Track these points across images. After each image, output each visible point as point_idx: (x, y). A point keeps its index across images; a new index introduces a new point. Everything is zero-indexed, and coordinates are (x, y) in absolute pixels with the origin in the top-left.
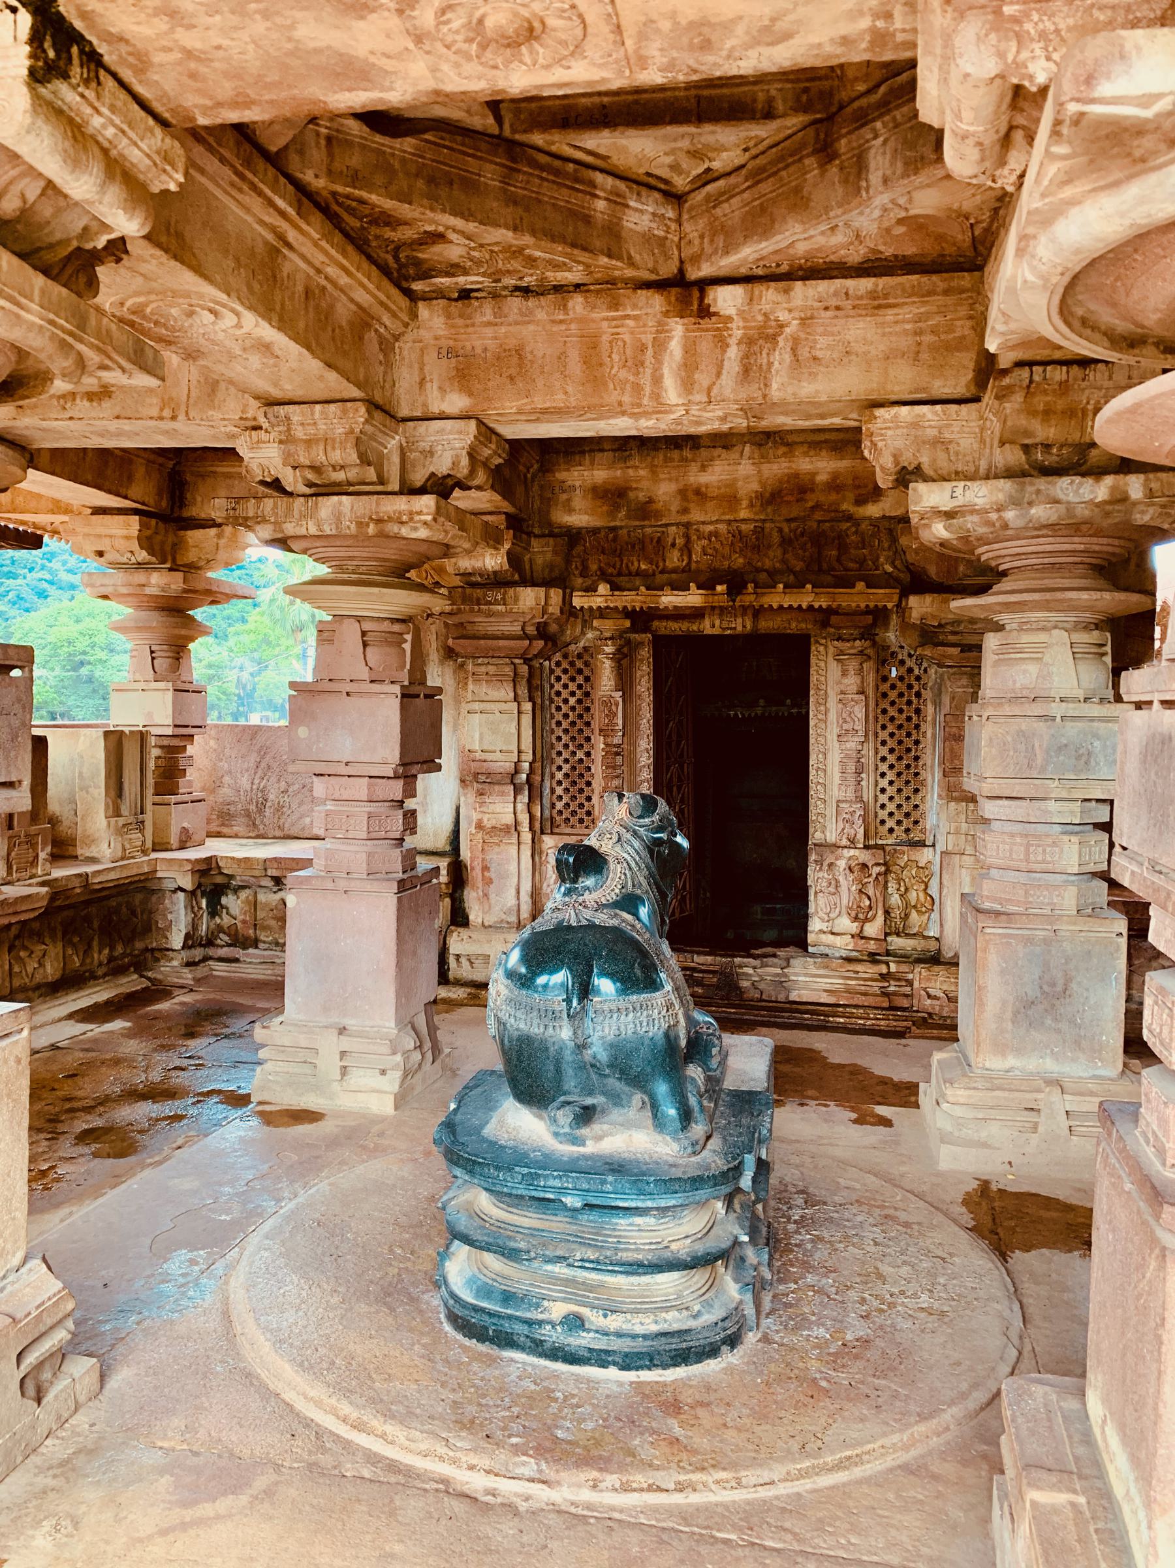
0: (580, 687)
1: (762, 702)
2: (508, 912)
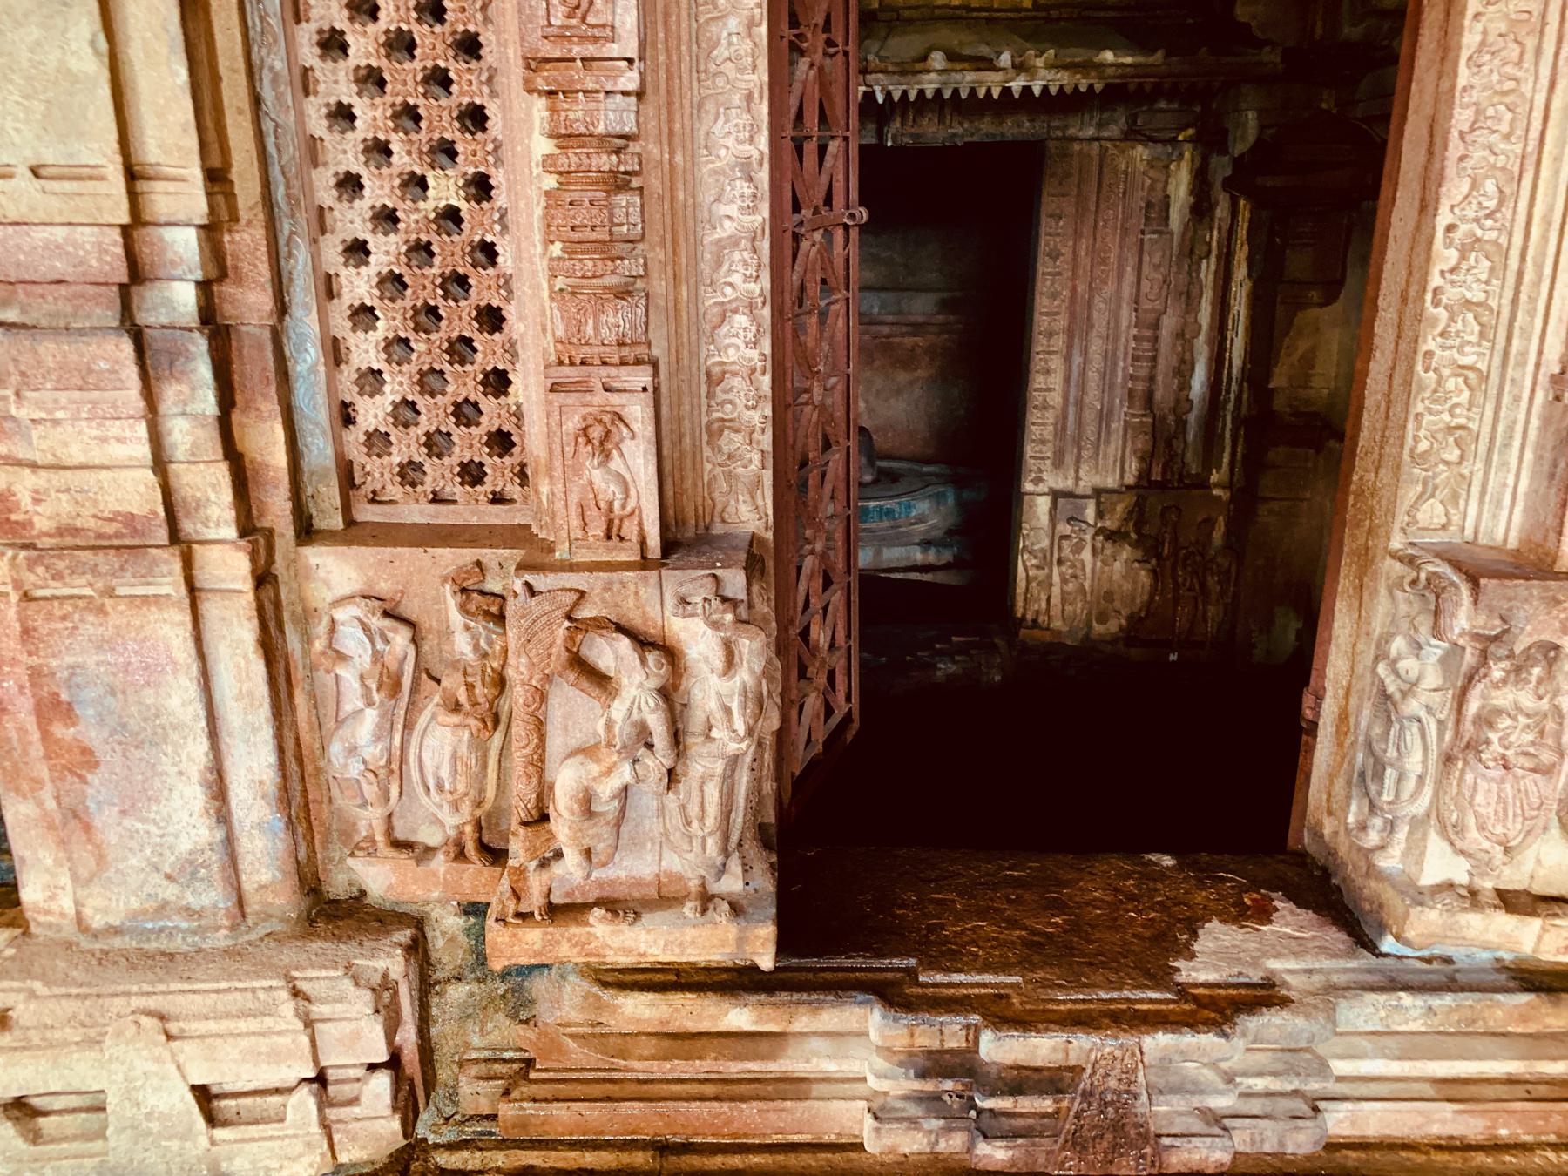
1: (937, 60)
2: (188, 871)
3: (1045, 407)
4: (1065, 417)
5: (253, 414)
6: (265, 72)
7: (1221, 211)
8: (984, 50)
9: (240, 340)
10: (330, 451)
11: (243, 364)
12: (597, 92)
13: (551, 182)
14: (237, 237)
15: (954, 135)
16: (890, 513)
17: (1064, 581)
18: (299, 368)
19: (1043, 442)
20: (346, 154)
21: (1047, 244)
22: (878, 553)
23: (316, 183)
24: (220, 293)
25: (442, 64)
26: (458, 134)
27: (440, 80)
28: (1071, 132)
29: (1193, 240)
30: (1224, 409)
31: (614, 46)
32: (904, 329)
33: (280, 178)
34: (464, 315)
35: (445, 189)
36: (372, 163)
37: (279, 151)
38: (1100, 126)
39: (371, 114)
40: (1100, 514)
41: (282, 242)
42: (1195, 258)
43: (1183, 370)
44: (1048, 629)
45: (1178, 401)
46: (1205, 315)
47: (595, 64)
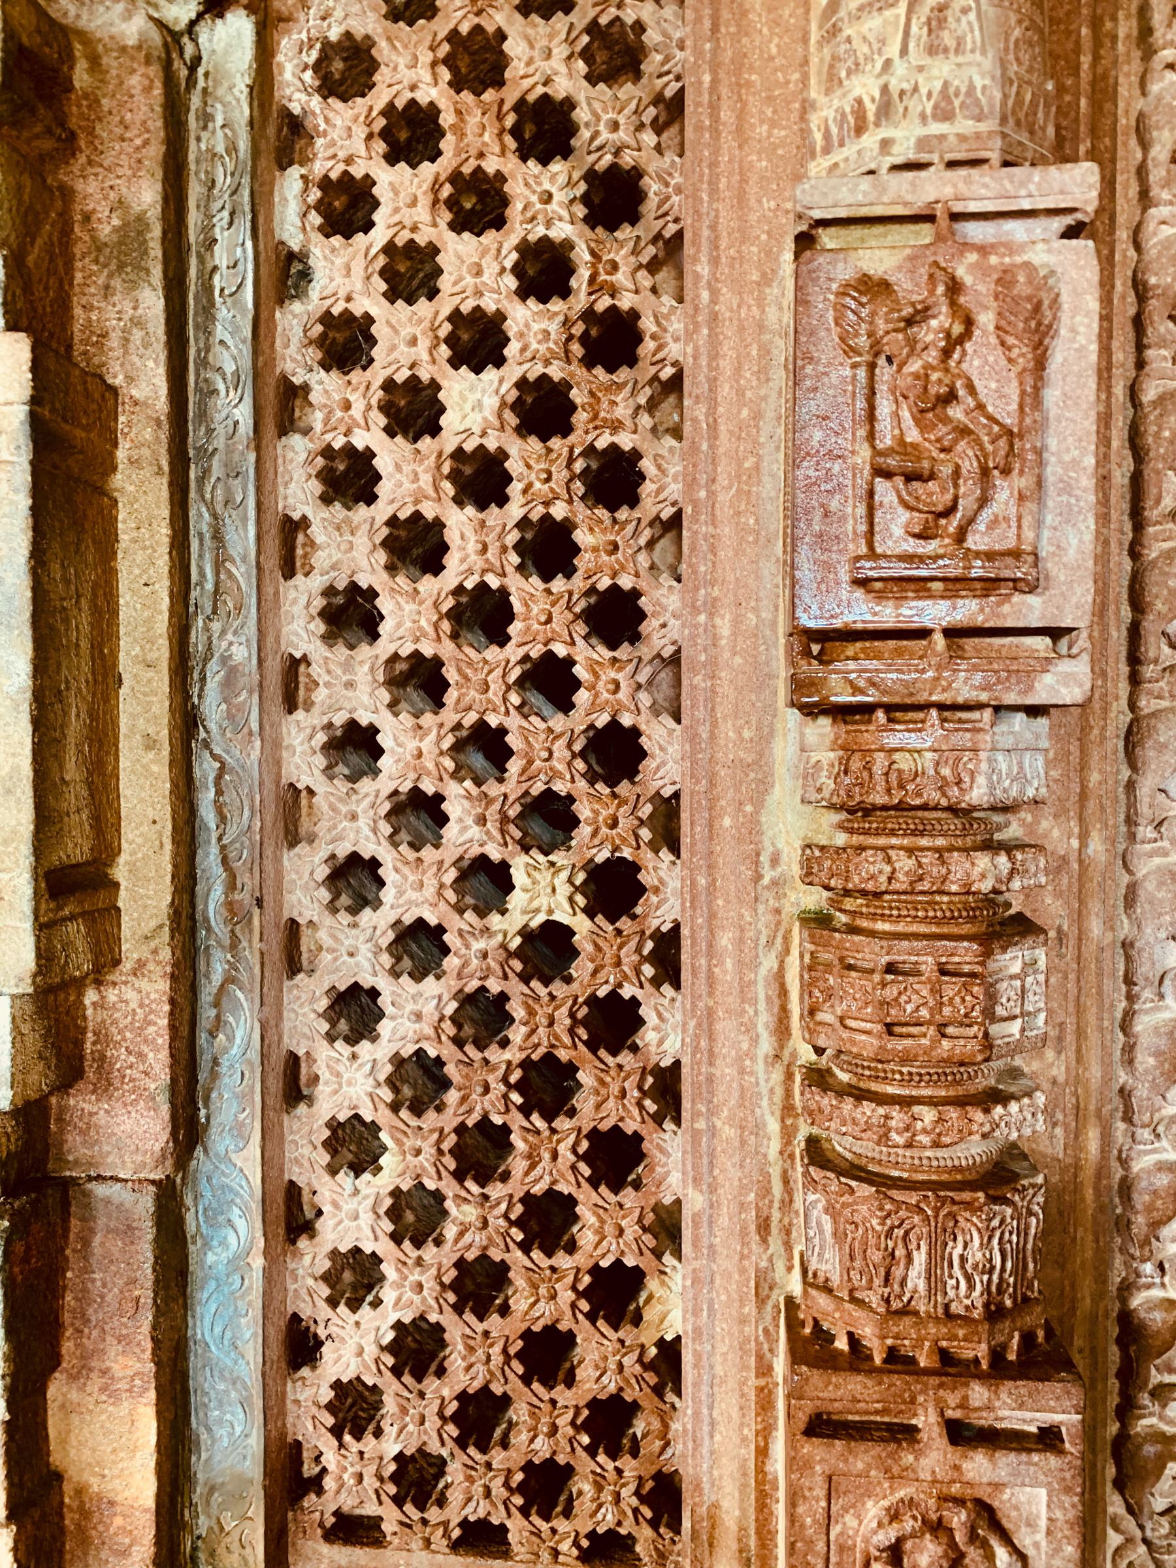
0: (543, 272)
5: (95, 1383)
6: (213, 665)
9: (88, 1218)
10: (255, 1443)
11: (87, 1270)
12: (980, 706)
13: (814, 898)
14: (112, 995)
18: (210, 1258)
20: (353, 820)
23: (290, 877)
24: (62, 1110)
25: (561, 650)
26: (582, 784)
27: (551, 680)
31: (1031, 599)
33: (218, 870)
34: (564, 1149)
35: (544, 891)
36: (404, 836)
37: (222, 819)
39: (412, 745)
41: (206, 995)
47: (970, 643)
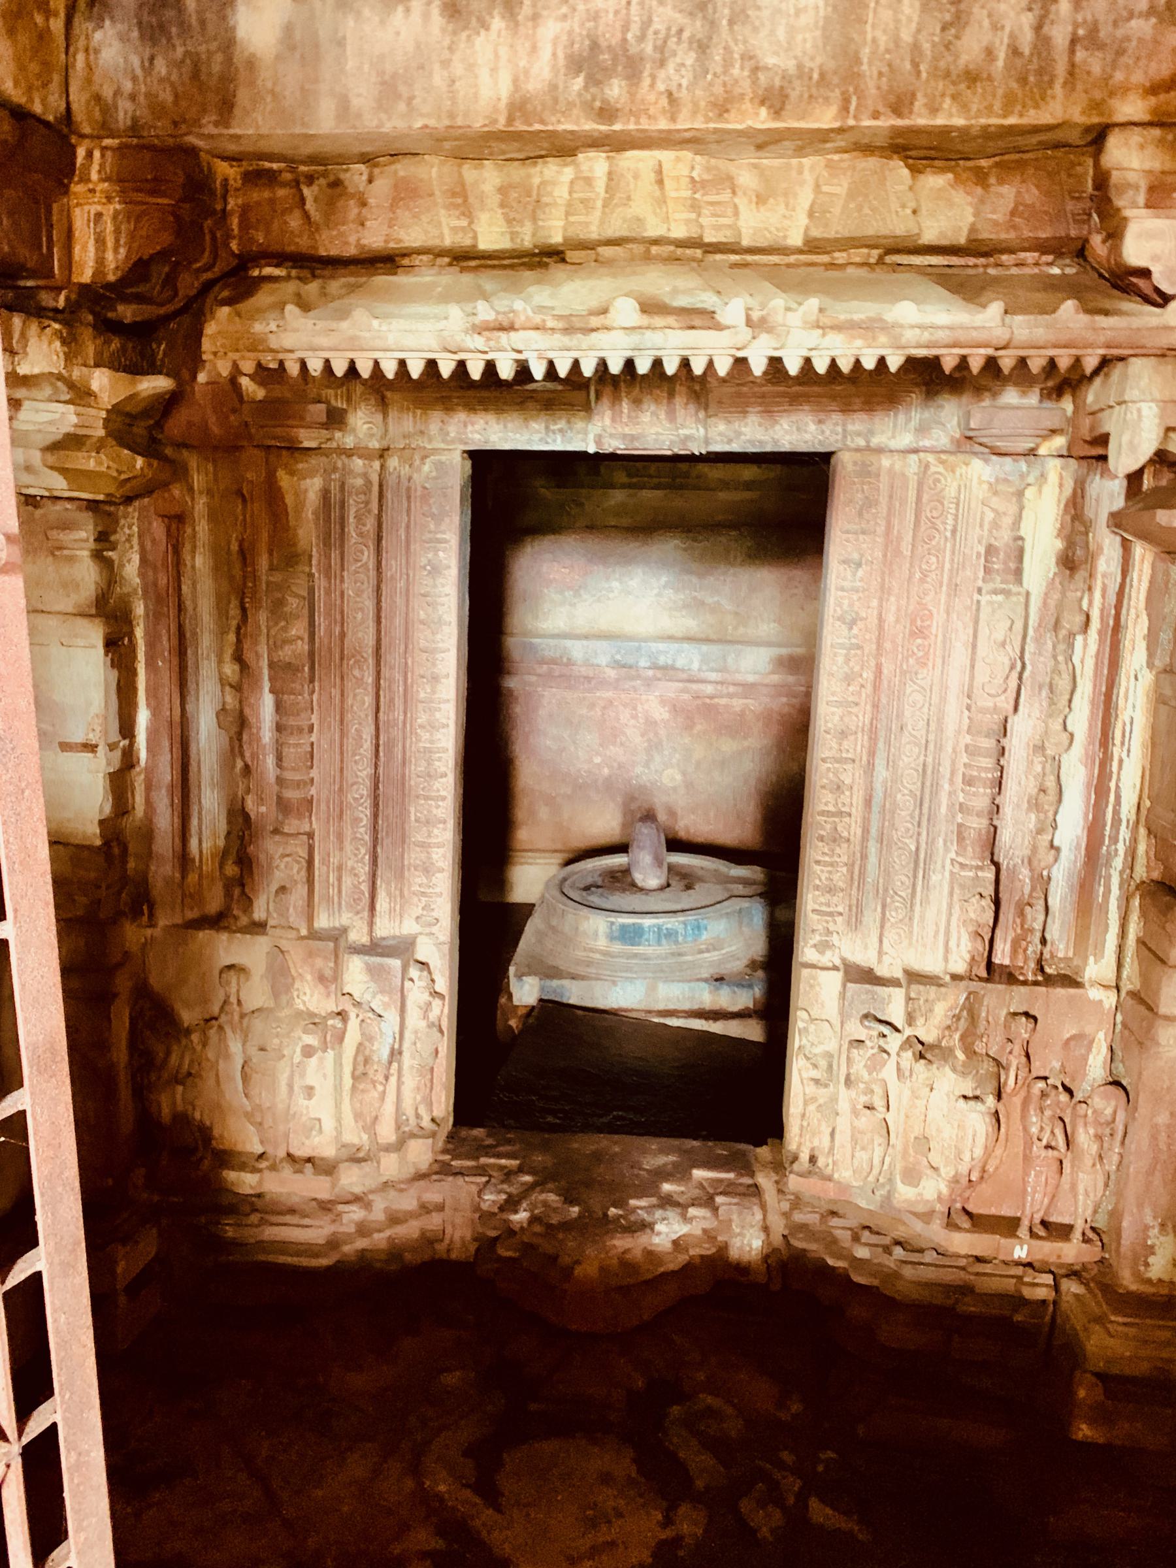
1: (626, 311)
3: (836, 838)
4: (864, 857)
7: (1108, 561)
8: (707, 300)
15: (688, 438)
16: (671, 935)
17: (855, 1113)
19: (831, 890)
21: (840, 605)
22: (652, 989)
28: (875, 441)
29: (1060, 607)
30: (1108, 865)
32: (731, 689)
38: (922, 430)
40: (910, 1019)
42: (1063, 633)
43: (1048, 796)
44: (829, 1179)
45: (1034, 849)
46: (1081, 718)
